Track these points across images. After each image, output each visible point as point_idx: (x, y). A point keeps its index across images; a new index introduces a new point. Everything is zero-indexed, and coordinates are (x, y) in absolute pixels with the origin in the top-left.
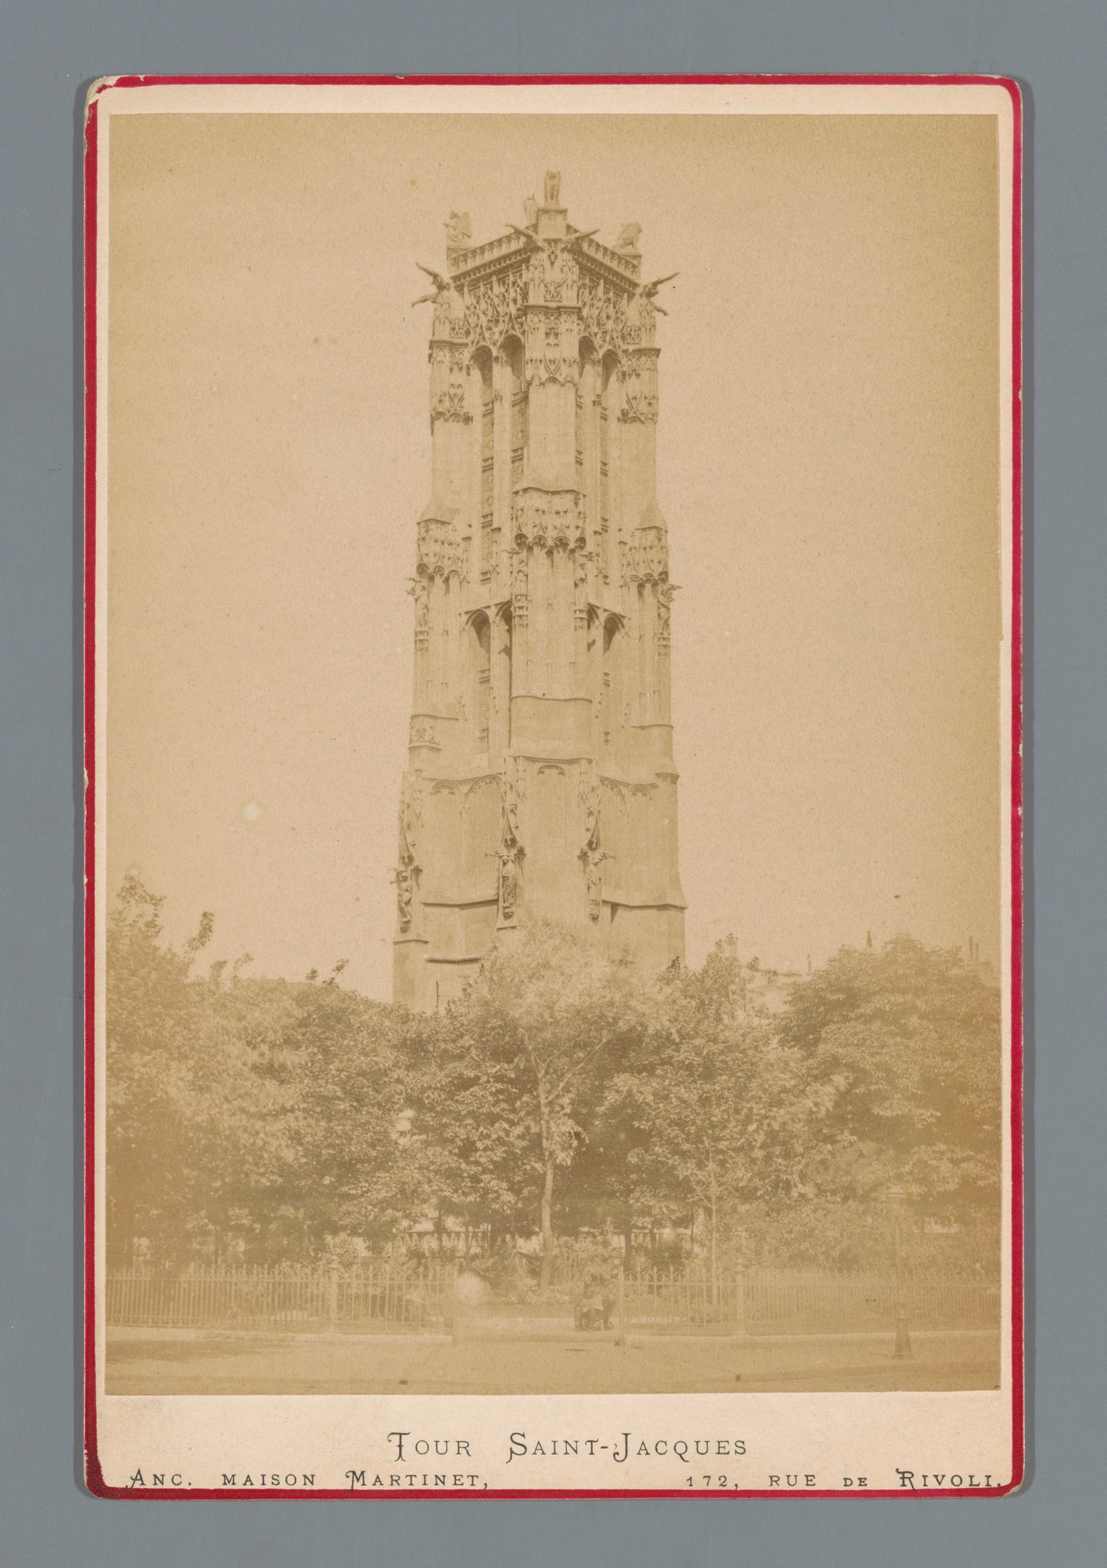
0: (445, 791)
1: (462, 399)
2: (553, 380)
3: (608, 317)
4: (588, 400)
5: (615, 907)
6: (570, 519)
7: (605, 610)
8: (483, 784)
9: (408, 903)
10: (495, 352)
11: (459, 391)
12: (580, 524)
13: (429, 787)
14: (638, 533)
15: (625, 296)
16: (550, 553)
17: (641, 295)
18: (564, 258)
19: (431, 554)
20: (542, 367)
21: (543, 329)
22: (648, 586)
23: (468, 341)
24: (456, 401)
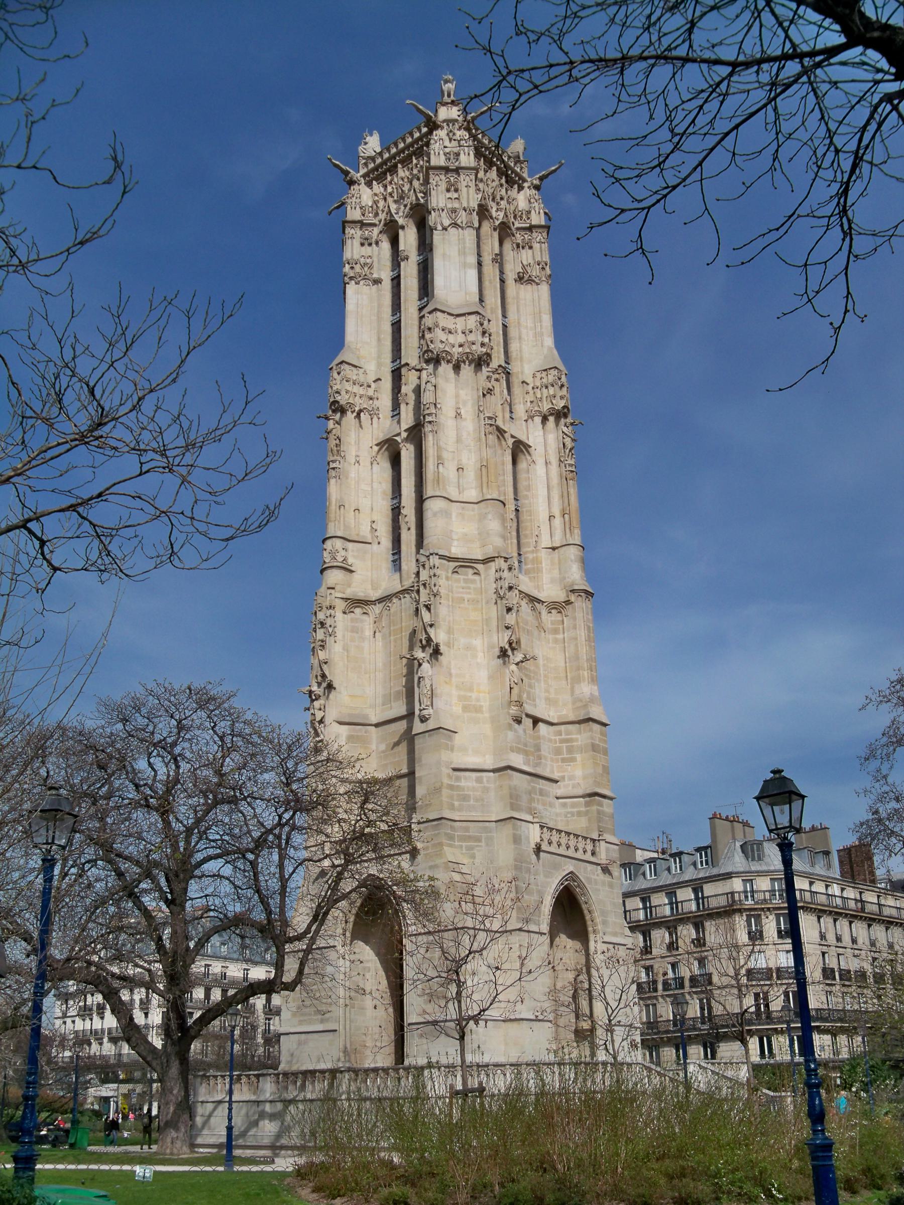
0: (358, 611)
1: (371, 267)
2: (455, 225)
4: (487, 259)
5: (536, 721)
6: (476, 337)
7: (512, 436)
8: (395, 600)
9: (321, 721)
10: (401, 221)
11: (369, 261)
12: (486, 340)
13: (341, 605)
14: (538, 375)
15: (516, 186)
16: (457, 368)
17: (529, 187)
19: (343, 393)
20: (444, 214)
21: (443, 186)
22: (552, 419)
23: (376, 221)
24: (366, 269)
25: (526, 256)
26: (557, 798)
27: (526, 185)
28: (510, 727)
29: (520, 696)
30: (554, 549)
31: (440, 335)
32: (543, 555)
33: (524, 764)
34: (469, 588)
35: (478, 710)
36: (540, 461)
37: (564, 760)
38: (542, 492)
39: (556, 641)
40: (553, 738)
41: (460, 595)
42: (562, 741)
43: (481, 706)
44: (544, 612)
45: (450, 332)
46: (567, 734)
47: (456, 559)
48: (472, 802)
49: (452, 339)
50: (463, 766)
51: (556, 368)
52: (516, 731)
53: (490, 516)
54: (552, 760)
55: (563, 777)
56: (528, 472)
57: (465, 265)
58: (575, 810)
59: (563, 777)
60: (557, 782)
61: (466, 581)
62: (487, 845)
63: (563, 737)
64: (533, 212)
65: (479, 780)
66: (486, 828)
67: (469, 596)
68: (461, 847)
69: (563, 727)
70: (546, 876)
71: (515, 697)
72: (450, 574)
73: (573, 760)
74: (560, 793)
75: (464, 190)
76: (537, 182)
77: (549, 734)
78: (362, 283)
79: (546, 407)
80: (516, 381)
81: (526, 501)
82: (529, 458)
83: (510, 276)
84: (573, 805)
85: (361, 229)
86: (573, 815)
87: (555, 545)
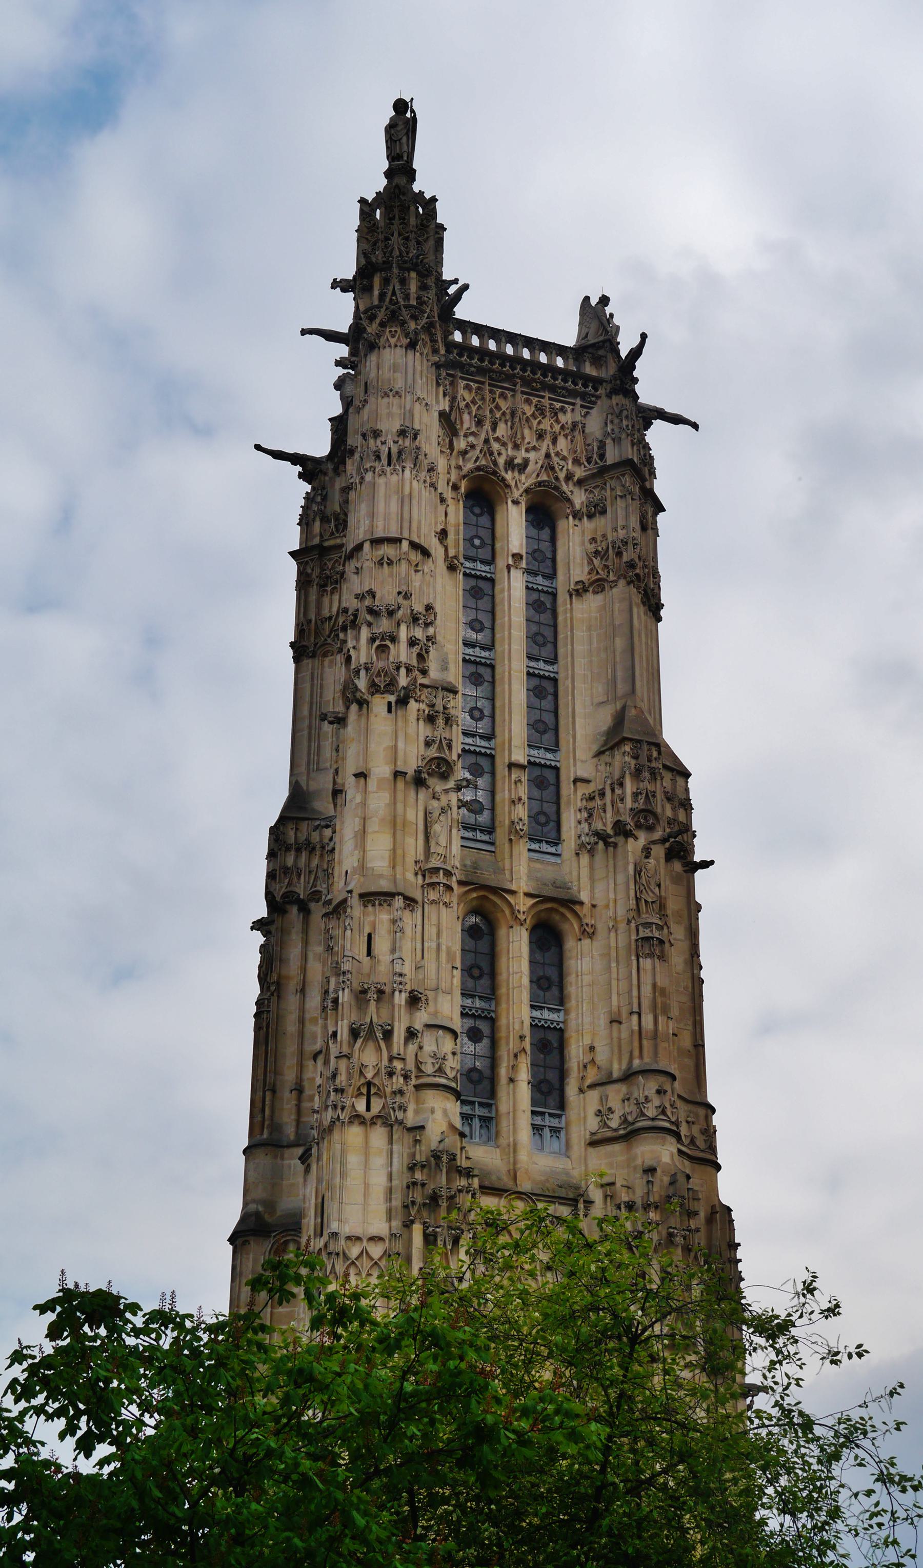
3: (540, 436)
27: (601, 391)
64: (609, 441)
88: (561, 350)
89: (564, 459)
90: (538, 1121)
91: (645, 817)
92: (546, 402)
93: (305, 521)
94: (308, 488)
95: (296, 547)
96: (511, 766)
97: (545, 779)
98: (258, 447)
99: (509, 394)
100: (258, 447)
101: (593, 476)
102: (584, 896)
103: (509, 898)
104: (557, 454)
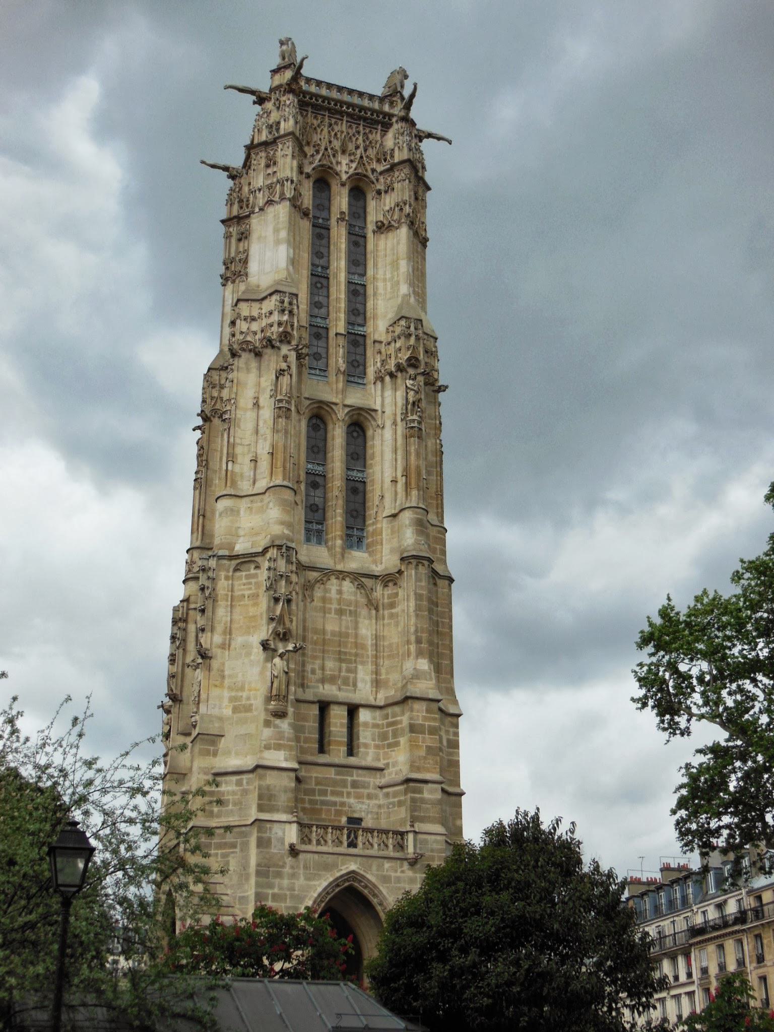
2: (270, 202)
3: (357, 147)
14: (391, 329)
15: (379, 127)
17: (397, 122)
18: (289, 99)
21: (263, 162)
25: (389, 201)
26: (381, 788)
27: (394, 120)
28: (267, 724)
29: (279, 689)
30: (394, 516)
31: (242, 326)
32: (384, 526)
33: (286, 760)
34: (250, 583)
35: (248, 709)
36: (388, 423)
37: (390, 746)
38: (388, 455)
39: (392, 616)
40: (380, 722)
41: (240, 593)
42: (390, 725)
43: (251, 705)
44: (379, 588)
45: (253, 319)
46: (393, 717)
47: (237, 557)
48: (230, 807)
49: (255, 326)
50: (223, 770)
51: (403, 317)
52: (276, 726)
53: (271, 505)
54: (377, 747)
55: (388, 764)
56: (373, 438)
57: (278, 242)
58: (396, 800)
59: (388, 764)
60: (382, 770)
61: (248, 577)
62: (242, 850)
63: (390, 720)
64: (396, 148)
65: (239, 783)
66: (242, 832)
67: (251, 592)
68: (217, 855)
69: (389, 710)
70: (308, 879)
71: (274, 692)
72: (231, 574)
73: (397, 744)
74: (383, 781)
75: (280, 161)
76: (402, 114)
77: (374, 718)
78: (237, 281)
79: (391, 365)
80: (369, 342)
81: (371, 471)
82: (373, 423)
83: (371, 227)
84: (395, 795)
85: (238, 223)
86: (394, 806)
87: (393, 512)
88: (371, 97)
89: (371, 159)
90: (349, 532)
91: (413, 362)
92: (361, 128)
93: (230, 203)
94: (231, 183)
95: (224, 217)
96: (337, 334)
97: (356, 341)
98: (203, 162)
99: (340, 122)
100: (203, 162)
101: (387, 171)
102: (378, 407)
103: (333, 407)
104: (367, 157)
